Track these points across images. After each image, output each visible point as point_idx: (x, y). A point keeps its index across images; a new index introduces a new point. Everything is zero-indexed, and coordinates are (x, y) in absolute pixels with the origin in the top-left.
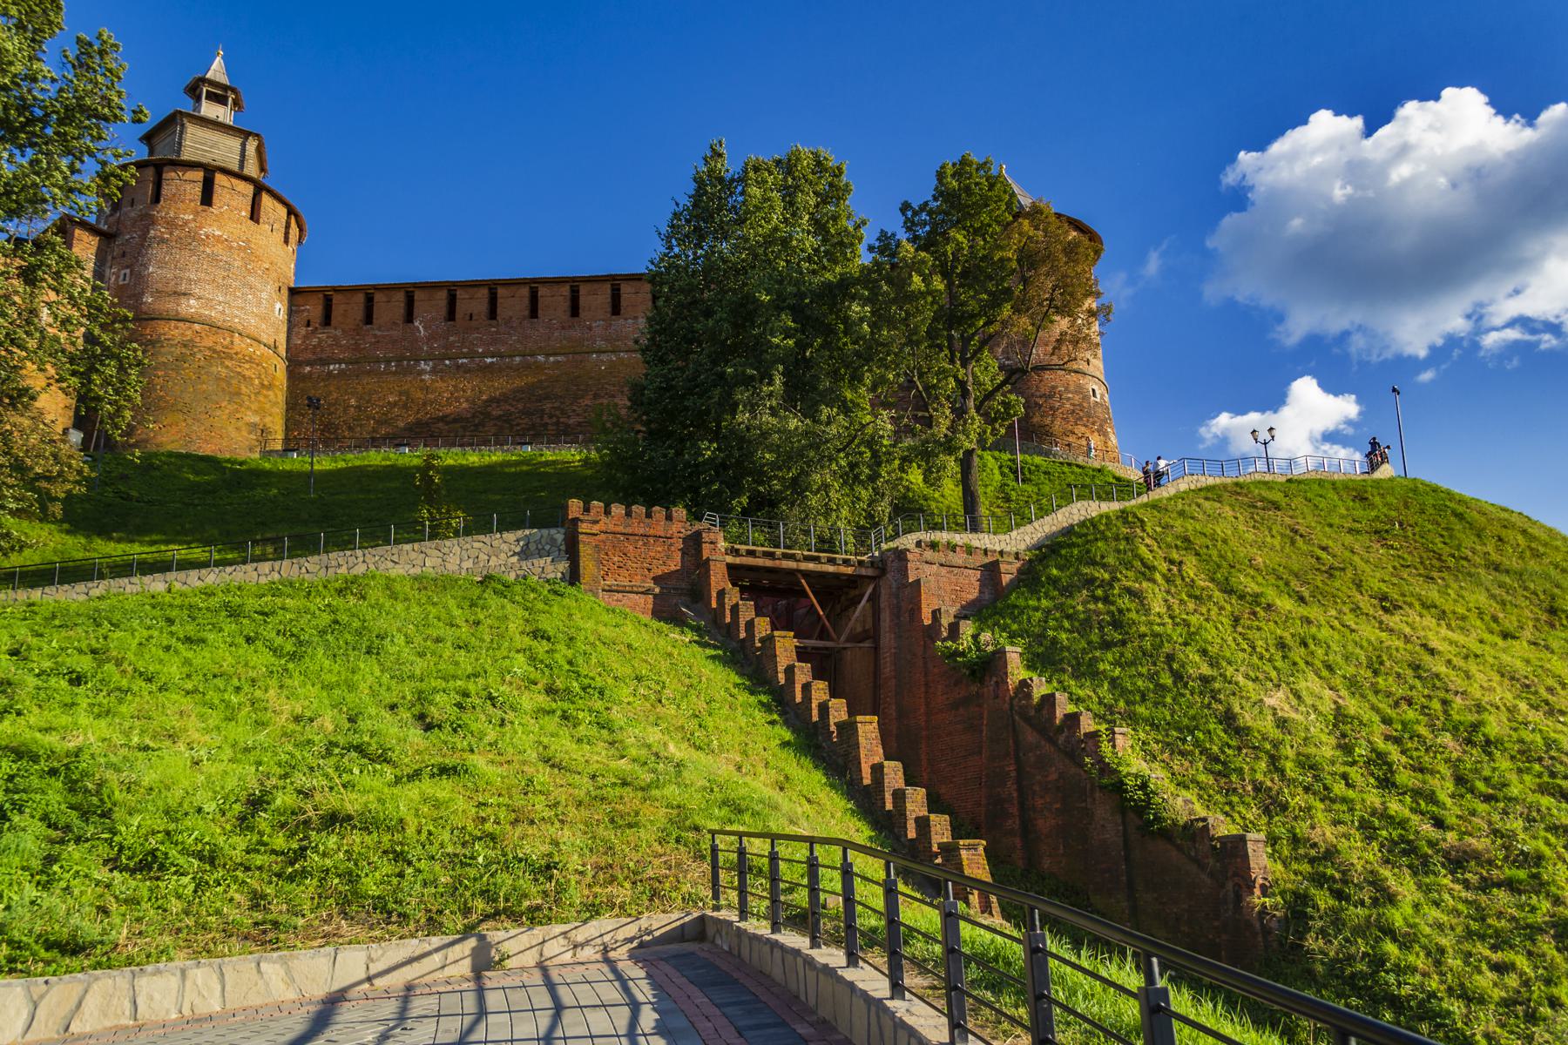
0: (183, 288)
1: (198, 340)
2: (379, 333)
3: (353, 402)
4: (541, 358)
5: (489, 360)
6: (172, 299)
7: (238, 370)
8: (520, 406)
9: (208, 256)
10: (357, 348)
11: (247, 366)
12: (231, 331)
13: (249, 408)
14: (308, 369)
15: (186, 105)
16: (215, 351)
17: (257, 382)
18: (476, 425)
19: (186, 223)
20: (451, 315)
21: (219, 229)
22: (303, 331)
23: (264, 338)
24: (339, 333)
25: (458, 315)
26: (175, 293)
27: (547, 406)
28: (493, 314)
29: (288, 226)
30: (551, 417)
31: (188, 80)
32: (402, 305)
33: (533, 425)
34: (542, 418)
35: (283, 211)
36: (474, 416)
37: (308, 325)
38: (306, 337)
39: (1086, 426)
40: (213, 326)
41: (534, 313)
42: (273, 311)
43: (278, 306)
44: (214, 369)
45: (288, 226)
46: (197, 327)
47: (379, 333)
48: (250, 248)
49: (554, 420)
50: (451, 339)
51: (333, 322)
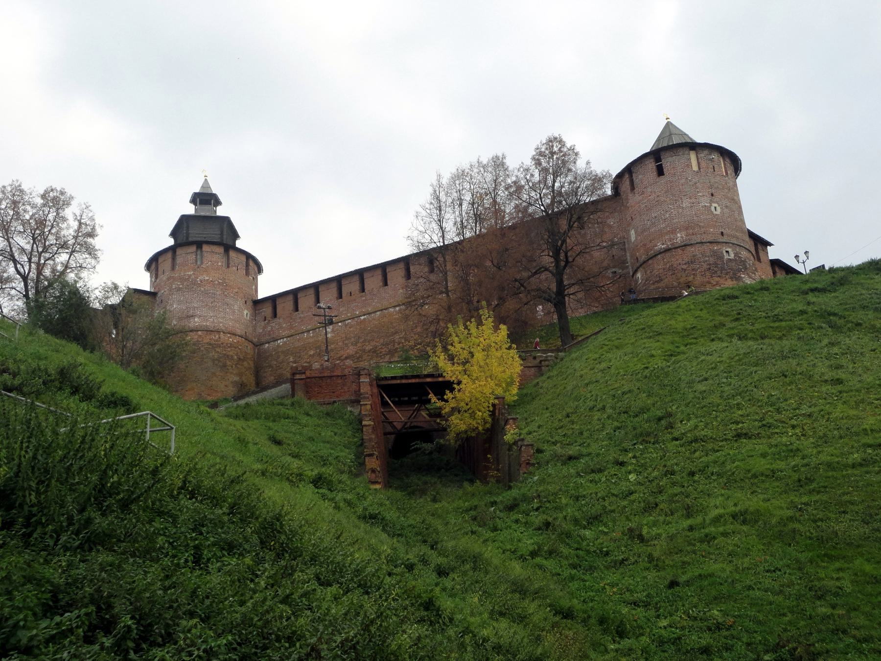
0: (191, 312)
1: (200, 340)
2: (302, 315)
3: (291, 359)
4: (391, 310)
5: (362, 318)
6: (186, 320)
7: (224, 352)
8: (382, 340)
9: (202, 292)
10: (291, 328)
11: (229, 349)
12: (218, 332)
13: (231, 373)
14: (267, 345)
15: (190, 210)
16: (210, 344)
17: (236, 357)
18: (358, 358)
19: (190, 276)
20: (340, 296)
21: (207, 276)
22: (263, 324)
23: (239, 332)
24: (281, 320)
25: (343, 295)
26: (188, 317)
27: (397, 337)
28: (363, 290)
29: (247, 265)
30: (399, 344)
31: (189, 197)
32: (313, 295)
33: (389, 351)
34: (394, 346)
35: (243, 258)
36: (356, 353)
37: (265, 320)
38: (264, 328)
39: (719, 276)
40: (209, 331)
41: (386, 284)
42: (243, 316)
43: (245, 312)
44: (211, 354)
45: (247, 265)
46: (200, 333)
47: (302, 315)
48: (225, 283)
49: (401, 345)
50: (341, 309)
51: (278, 316)
